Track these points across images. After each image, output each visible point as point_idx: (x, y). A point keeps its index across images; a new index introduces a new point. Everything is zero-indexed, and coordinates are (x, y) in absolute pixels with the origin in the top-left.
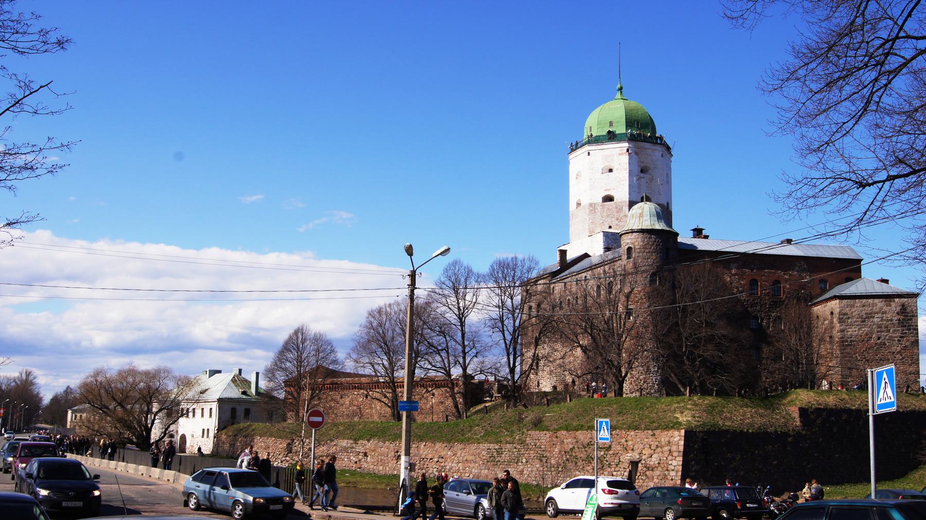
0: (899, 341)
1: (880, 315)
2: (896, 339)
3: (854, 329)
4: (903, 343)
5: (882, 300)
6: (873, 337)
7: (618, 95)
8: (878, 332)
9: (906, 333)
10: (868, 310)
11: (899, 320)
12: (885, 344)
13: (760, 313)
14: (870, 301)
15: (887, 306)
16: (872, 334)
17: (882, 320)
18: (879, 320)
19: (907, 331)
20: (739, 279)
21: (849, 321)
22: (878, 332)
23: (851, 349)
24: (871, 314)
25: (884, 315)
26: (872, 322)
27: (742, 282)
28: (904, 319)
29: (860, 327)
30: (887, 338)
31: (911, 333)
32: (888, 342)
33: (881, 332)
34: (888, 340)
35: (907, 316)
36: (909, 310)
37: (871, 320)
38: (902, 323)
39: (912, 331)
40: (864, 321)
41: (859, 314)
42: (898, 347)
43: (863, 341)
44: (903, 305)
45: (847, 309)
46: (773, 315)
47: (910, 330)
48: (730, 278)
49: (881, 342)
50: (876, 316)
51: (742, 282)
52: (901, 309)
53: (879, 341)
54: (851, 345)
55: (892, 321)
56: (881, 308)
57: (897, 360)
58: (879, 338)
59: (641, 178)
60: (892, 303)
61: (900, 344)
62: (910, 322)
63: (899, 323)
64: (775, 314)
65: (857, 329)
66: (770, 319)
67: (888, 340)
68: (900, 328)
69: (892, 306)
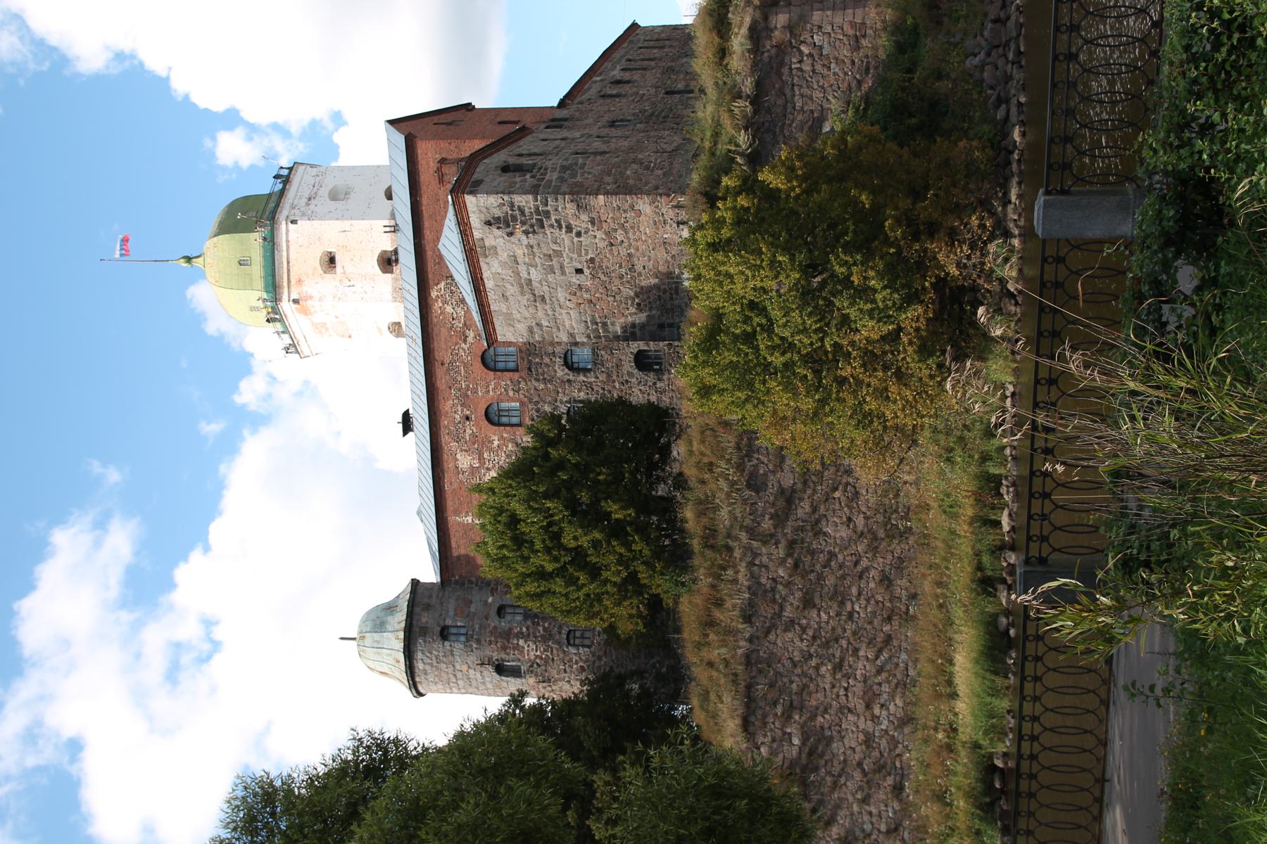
0: (579, 234)
1: (522, 269)
2: (576, 239)
3: (565, 316)
4: (584, 225)
5: (482, 264)
6: (578, 282)
7: (198, 263)
8: (563, 273)
9: (558, 221)
10: (512, 290)
11: (526, 233)
12: (592, 260)
13: (558, 404)
14: (489, 284)
15: (497, 253)
16: (570, 284)
17: (532, 266)
18: (533, 271)
19: (553, 218)
20: (490, 450)
21: (545, 323)
22: (563, 273)
23: (613, 324)
24: (522, 287)
25: (520, 260)
26: (540, 283)
27: (496, 443)
28: (523, 223)
29: (557, 307)
30: (575, 256)
31: (556, 210)
32: (587, 254)
33: (562, 267)
34: (580, 255)
35: (514, 218)
36: (498, 213)
37: (535, 284)
38: (532, 226)
39: (549, 208)
40: (543, 298)
41: (527, 307)
42: (595, 237)
43: (590, 302)
44: (489, 223)
45: (518, 326)
46: (560, 374)
47: (548, 212)
48: (488, 469)
49: (589, 268)
50: (524, 275)
51: (496, 443)
52: (499, 228)
53: (587, 271)
54: (605, 324)
55: (532, 247)
56: (503, 264)
57: (629, 238)
58: (579, 271)
59: (344, 273)
60: (487, 244)
61: (586, 232)
62: (527, 210)
63: (534, 232)
64: (556, 368)
65: (564, 312)
66: (569, 381)
67: (580, 255)
68: (548, 232)
69: (493, 243)
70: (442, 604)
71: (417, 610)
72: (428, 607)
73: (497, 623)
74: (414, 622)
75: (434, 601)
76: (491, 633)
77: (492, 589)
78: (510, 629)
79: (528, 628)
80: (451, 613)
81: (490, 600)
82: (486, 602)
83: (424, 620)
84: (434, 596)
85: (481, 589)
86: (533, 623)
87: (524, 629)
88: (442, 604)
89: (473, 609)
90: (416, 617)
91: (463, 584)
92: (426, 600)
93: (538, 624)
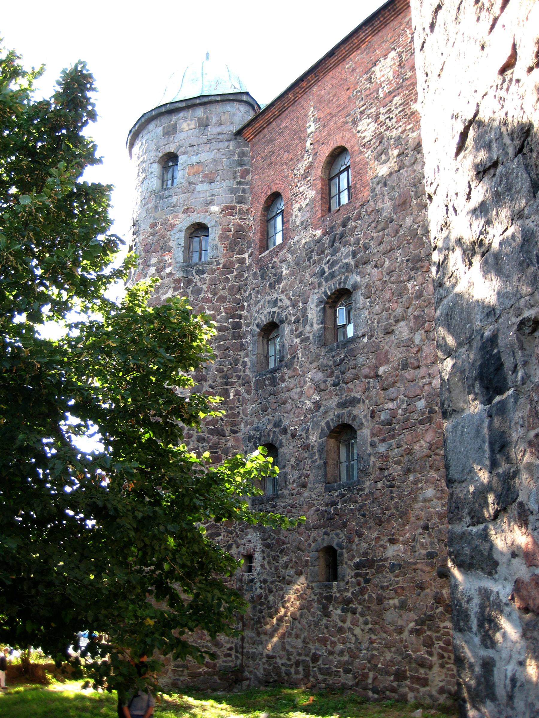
70: (209, 142)
71: (200, 112)
72: (204, 125)
73: (178, 227)
74: (181, 115)
75: (213, 130)
76: (165, 223)
77: (234, 208)
78: (170, 249)
79: (171, 274)
80: (194, 159)
81: (215, 209)
82: (211, 203)
83: (185, 126)
84: (219, 130)
85: (232, 191)
86: (178, 281)
87: (168, 270)
88: (209, 142)
89: (200, 187)
90: (188, 114)
91: (241, 164)
92: (214, 119)
93: (175, 289)
